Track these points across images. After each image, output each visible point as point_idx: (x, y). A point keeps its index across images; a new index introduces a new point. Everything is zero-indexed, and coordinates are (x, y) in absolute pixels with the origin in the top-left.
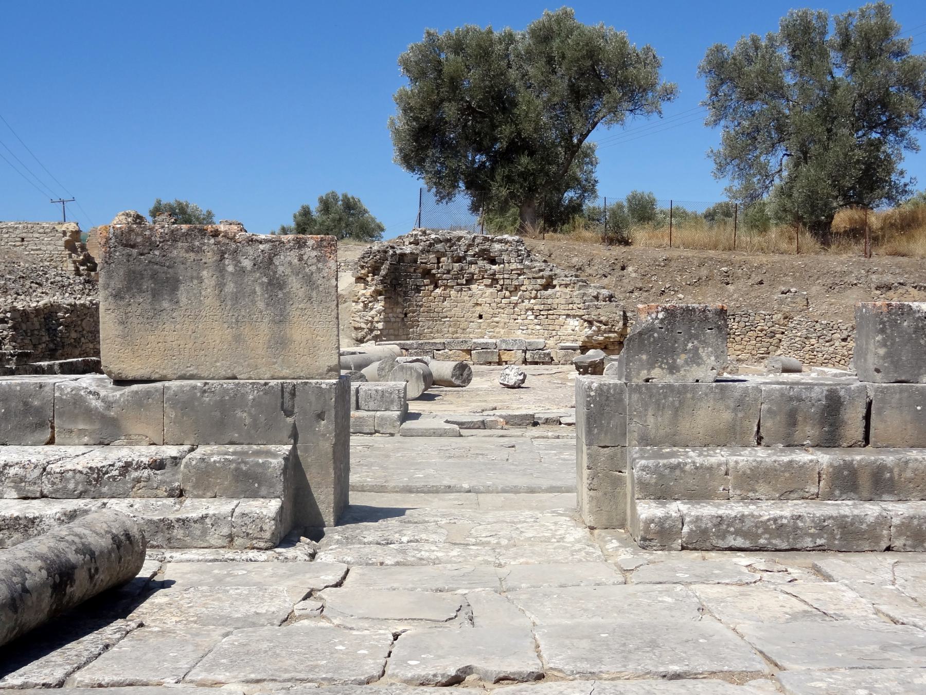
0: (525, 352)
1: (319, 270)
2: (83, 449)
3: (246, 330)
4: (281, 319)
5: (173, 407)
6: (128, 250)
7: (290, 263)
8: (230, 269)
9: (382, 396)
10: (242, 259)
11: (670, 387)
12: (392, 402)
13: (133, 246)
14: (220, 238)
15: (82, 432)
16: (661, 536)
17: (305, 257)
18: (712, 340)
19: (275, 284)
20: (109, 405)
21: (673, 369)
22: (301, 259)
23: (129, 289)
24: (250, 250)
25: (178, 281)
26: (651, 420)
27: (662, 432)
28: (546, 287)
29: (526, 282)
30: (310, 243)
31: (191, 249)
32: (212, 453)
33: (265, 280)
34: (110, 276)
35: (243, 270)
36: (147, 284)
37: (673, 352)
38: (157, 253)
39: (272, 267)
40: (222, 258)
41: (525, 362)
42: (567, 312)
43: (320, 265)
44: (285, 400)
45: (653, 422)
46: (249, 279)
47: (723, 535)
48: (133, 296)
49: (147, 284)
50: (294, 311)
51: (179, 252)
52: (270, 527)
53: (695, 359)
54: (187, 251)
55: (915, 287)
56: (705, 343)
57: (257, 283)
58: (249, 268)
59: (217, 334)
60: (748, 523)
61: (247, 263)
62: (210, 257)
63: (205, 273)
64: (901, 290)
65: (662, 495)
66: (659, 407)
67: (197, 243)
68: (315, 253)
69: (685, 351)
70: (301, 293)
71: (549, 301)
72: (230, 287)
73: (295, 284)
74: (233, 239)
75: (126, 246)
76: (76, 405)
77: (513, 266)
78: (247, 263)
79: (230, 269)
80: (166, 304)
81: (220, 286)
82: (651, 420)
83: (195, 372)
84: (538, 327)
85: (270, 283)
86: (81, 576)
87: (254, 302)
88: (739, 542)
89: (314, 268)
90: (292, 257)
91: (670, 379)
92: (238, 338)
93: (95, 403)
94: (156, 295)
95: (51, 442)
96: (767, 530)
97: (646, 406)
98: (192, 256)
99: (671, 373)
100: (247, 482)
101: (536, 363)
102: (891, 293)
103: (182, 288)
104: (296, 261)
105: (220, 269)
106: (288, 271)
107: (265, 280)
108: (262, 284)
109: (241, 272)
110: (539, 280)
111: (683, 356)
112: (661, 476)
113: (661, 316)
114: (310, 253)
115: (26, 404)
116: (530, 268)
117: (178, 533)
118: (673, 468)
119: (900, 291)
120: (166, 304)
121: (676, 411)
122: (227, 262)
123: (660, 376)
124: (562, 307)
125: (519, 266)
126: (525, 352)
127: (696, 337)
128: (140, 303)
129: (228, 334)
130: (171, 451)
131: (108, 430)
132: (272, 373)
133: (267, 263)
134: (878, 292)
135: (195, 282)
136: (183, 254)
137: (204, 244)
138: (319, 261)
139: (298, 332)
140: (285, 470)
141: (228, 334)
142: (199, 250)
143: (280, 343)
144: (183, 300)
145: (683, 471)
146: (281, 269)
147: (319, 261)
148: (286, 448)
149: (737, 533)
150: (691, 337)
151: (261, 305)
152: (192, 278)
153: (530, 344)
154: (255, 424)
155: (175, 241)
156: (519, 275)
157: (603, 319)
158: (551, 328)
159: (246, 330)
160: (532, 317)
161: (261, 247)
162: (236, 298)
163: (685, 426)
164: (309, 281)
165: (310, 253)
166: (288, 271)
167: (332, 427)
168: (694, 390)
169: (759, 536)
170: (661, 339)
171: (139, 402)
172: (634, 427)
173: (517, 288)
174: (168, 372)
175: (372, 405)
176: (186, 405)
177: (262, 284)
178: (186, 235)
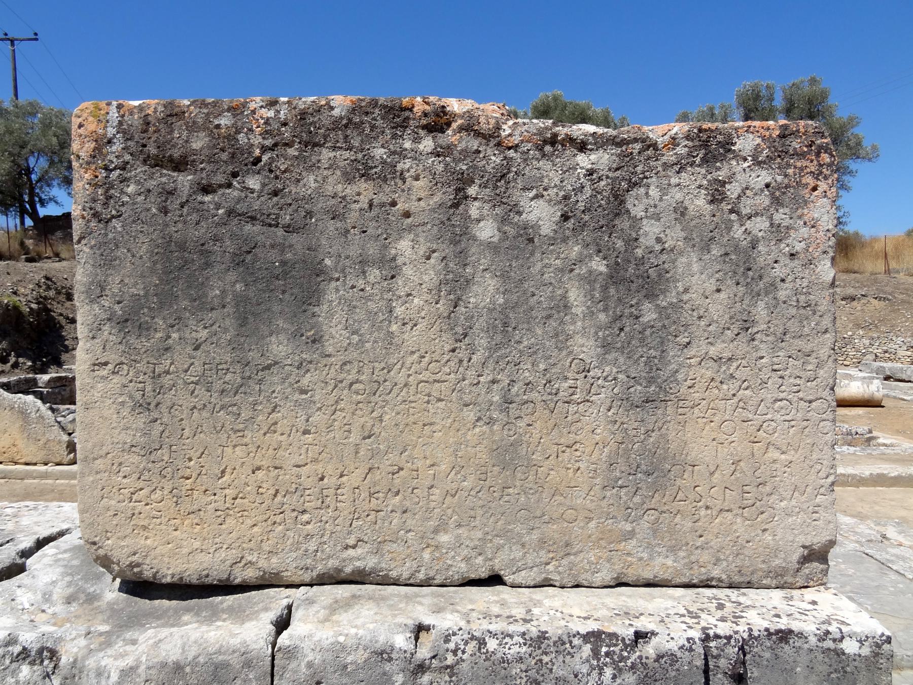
1: (779, 232)
4: (651, 394)
6: (165, 177)
7: (681, 211)
8: (487, 231)
10: (525, 200)
13: (180, 165)
14: (450, 136)
17: (733, 190)
19: (633, 279)
22: (717, 195)
23: (166, 299)
24: (549, 171)
25: (319, 272)
30: (745, 144)
31: (363, 170)
33: (599, 266)
34: (106, 260)
35: (528, 236)
36: (223, 284)
38: (254, 182)
39: (623, 224)
40: (460, 199)
43: (781, 216)
46: (548, 264)
48: (178, 322)
49: (223, 284)
50: (692, 370)
51: (322, 179)
54: (348, 178)
55: (876, 298)
57: (572, 278)
58: (546, 229)
59: (443, 441)
61: (541, 214)
62: (421, 195)
63: (404, 246)
64: (863, 301)
67: (379, 152)
68: (765, 176)
70: (718, 308)
72: (485, 291)
73: (697, 279)
74: (492, 136)
75: (157, 162)
78: (541, 214)
79: (487, 231)
80: (279, 347)
81: (455, 286)
83: (370, 563)
85: (615, 276)
87: (562, 339)
89: (759, 225)
90: (689, 189)
92: (508, 456)
94: (249, 318)
98: (365, 190)
102: (855, 303)
103: (332, 293)
104: (700, 203)
106: (675, 237)
107: (599, 266)
108: (590, 279)
119: (862, 301)
120: (279, 347)
122: (474, 210)
128: (200, 342)
129: (477, 440)
133: (603, 213)
134: (844, 302)
135: (374, 274)
136: (335, 185)
137: (401, 154)
138: (777, 202)
139: (706, 436)
141: (477, 440)
142: (388, 174)
144: (335, 333)
146: (650, 230)
147: (777, 202)
151: (585, 347)
152: (364, 263)
155: (312, 144)
159: (536, 430)
161: (584, 161)
162: (504, 325)
164: (743, 267)
165: (748, 179)
166: (675, 237)
174: (287, 563)
177: (590, 279)
178: (346, 124)
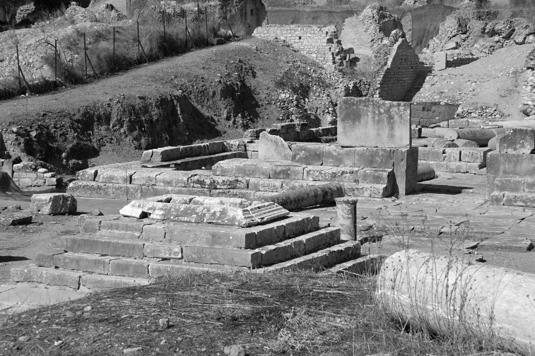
1: (404, 113)
2: (331, 167)
3: (381, 132)
4: (392, 128)
5: (358, 155)
8: (377, 112)
9: (472, 155)
11: (514, 155)
12: (477, 158)
15: (331, 162)
16: (497, 200)
18: (529, 140)
19: (391, 118)
20: (339, 154)
21: (515, 149)
26: (507, 166)
27: (510, 170)
30: (402, 104)
31: (365, 106)
32: (368, 170)
35: (381, 112)
37: (515, 143)
44: (391, 154)
45: (507, 166)
46: (382, 116)
47: (516, 201)
50: (396, 127)
52: (381, 191)
53: (523, 146)
56: (527, 141)
57: (385, 117)
60: (524, 198)
62: (370, 108)
63: (369, 113)
65: (502, 188)
66: (510, 162)
69: (519, 144)
72: (377, 118)
73: (396, 117)
76: (329, 155)
78: (382, 111)
79: (377, 112)
80: (357, 123)
81: (374, 118)
82: (507, 166)
86: (329, 194)
88: (521, 204)
90: (396, 109)
91: (514, 152)
92: (378, 135)
93: (334, 153)
94: (354, 121)
95: (322, 165)
96: (530, 201)
97: (505, 161)
98: (365, 108)
99: (515, 150)
100: (377, 179)
104: (397, 110)
105: (374, 113)
109: (380, 113)
111: (519, 145)
112: (503, 183)
113: (511, 132)
114: (402, 108)
115: (315, 153)
117: (356, 192)
118: (507, 181)
121: (516, 163)
123: (510, 151)
127: (523, 139)
130: (356, 169)
131: (338, 161)
132: (388, 145)
133: (388, 111)
136: (363, 107)
140: (388, 176)
142: (368, 106)
143: (392, 136)
144: (362, 121)
145: (510, 182)
148: (390, 170)
149: (521, 201)
150: (522, 139)
151: (386, 124)
154: (382, 162)
159: (381, 132)
163: (518, 168)
164: (401, 117)
165: (402, 108)
167: (405, 164)
168: (522, 156)
169: (528, 202)
170: (511, 139)
171: (348, 154)
172: (502, 167)
174: (357, 145)
175: (467, 159)
176: (361, 155)
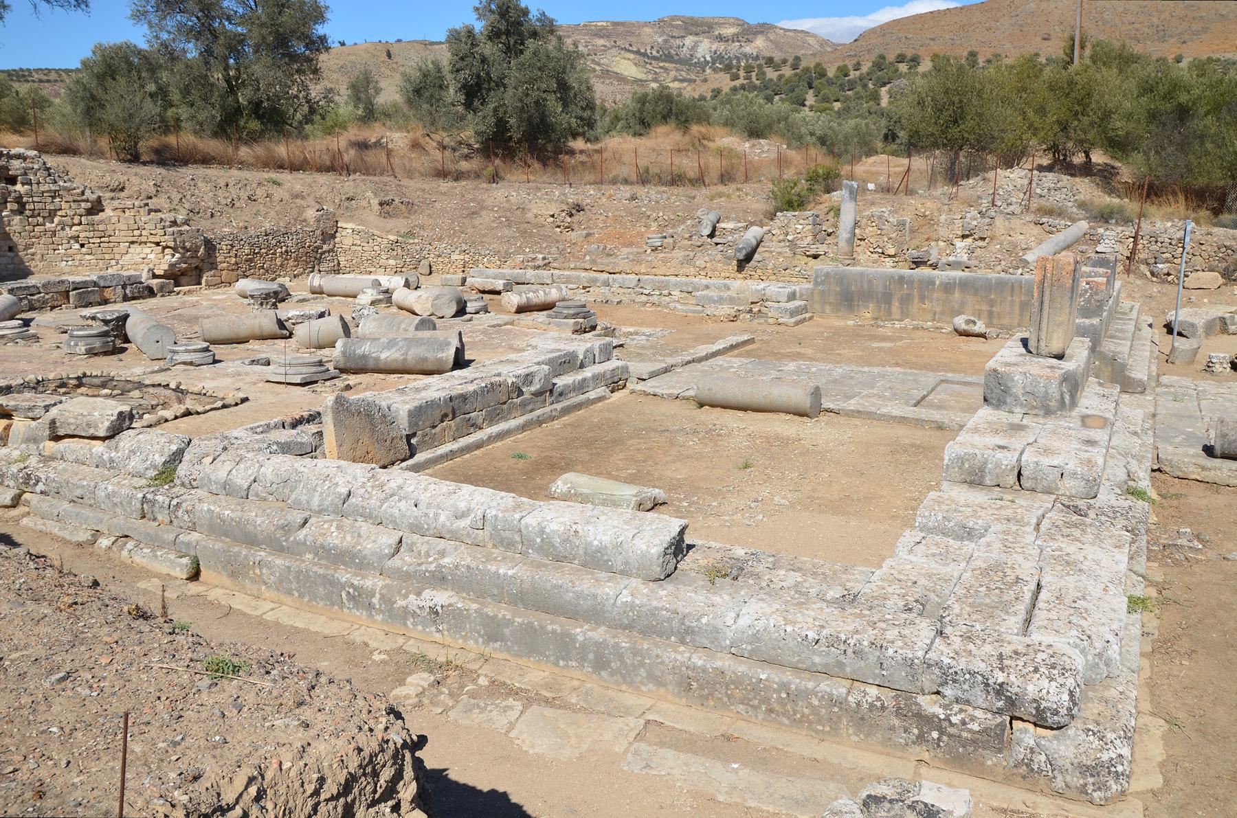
0: (124, 287)
28: (90, 212)
29: (64, 205)
41: (126, 299)
42: (131, 239)
71: (101, 227)
77: (46, 188)
84: (88, 257)
101: (134, 298)
110: (83, 204)
116: (69, 190)
124: (123, 233)
125: (53, 188)
126: (124, 287)
153: (129, 278)
156: (54, 197)
157: (188, 245)
158: (107, 256)
160: (77, 246)
173: (52, 214)
